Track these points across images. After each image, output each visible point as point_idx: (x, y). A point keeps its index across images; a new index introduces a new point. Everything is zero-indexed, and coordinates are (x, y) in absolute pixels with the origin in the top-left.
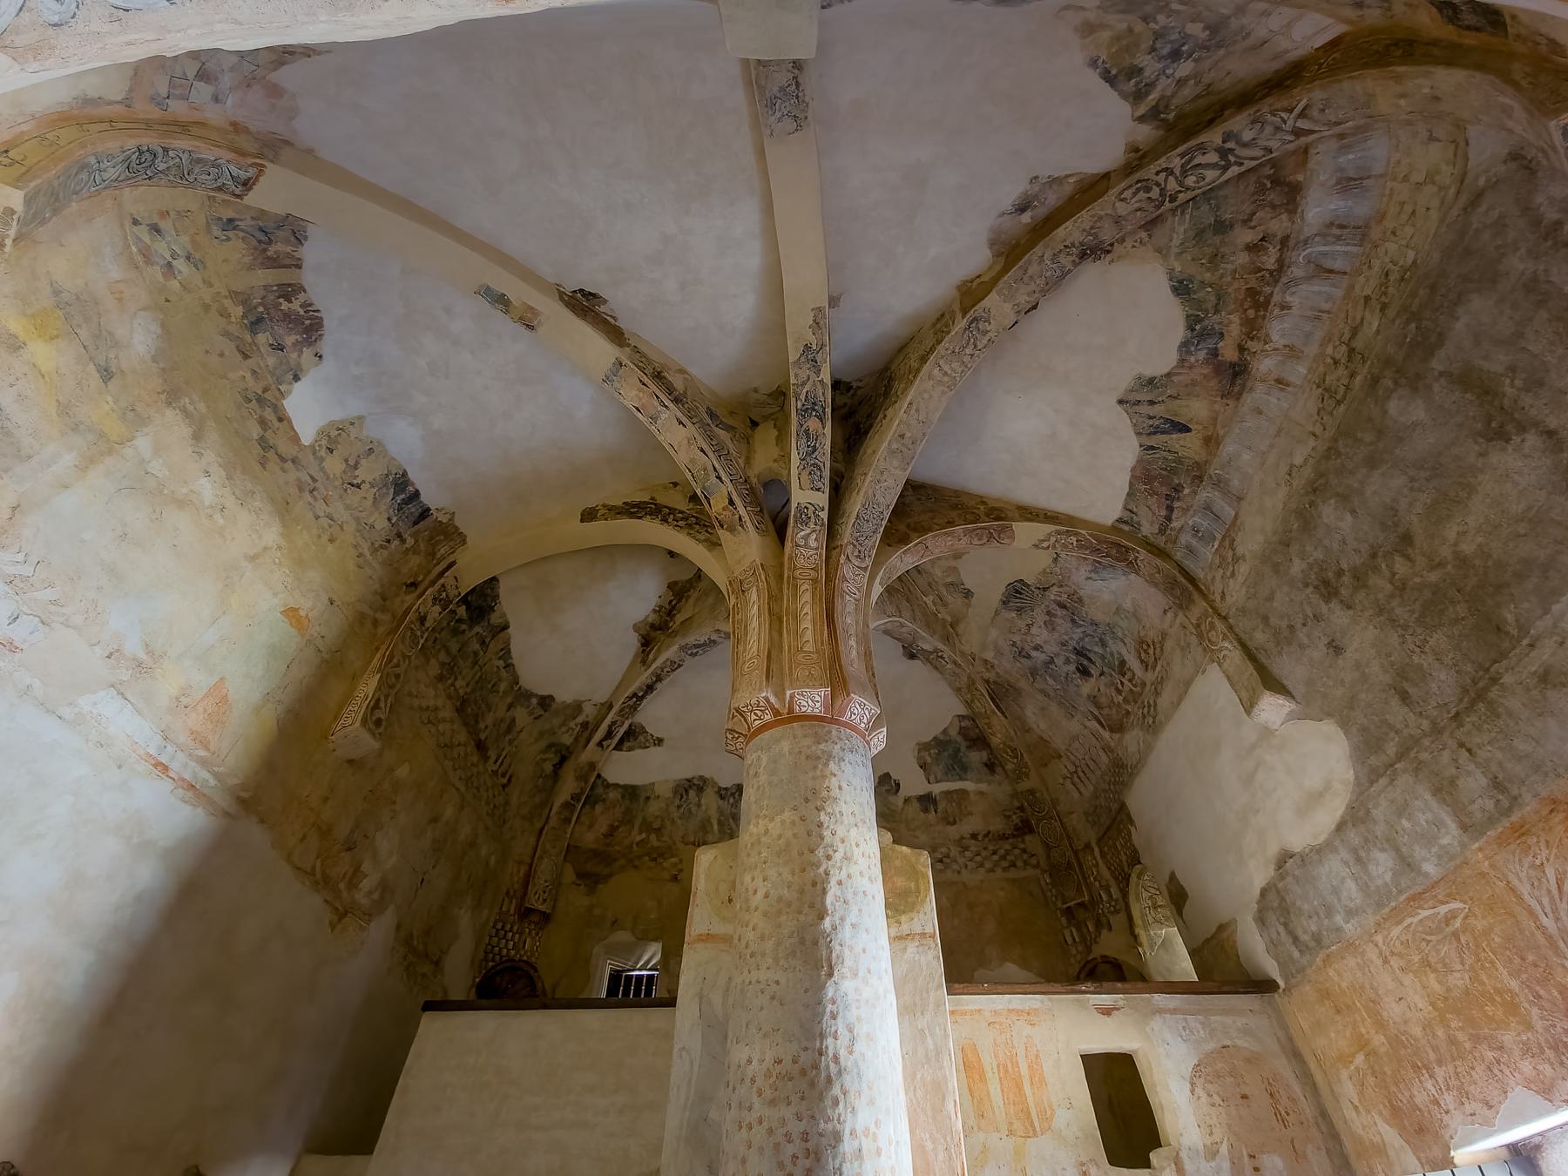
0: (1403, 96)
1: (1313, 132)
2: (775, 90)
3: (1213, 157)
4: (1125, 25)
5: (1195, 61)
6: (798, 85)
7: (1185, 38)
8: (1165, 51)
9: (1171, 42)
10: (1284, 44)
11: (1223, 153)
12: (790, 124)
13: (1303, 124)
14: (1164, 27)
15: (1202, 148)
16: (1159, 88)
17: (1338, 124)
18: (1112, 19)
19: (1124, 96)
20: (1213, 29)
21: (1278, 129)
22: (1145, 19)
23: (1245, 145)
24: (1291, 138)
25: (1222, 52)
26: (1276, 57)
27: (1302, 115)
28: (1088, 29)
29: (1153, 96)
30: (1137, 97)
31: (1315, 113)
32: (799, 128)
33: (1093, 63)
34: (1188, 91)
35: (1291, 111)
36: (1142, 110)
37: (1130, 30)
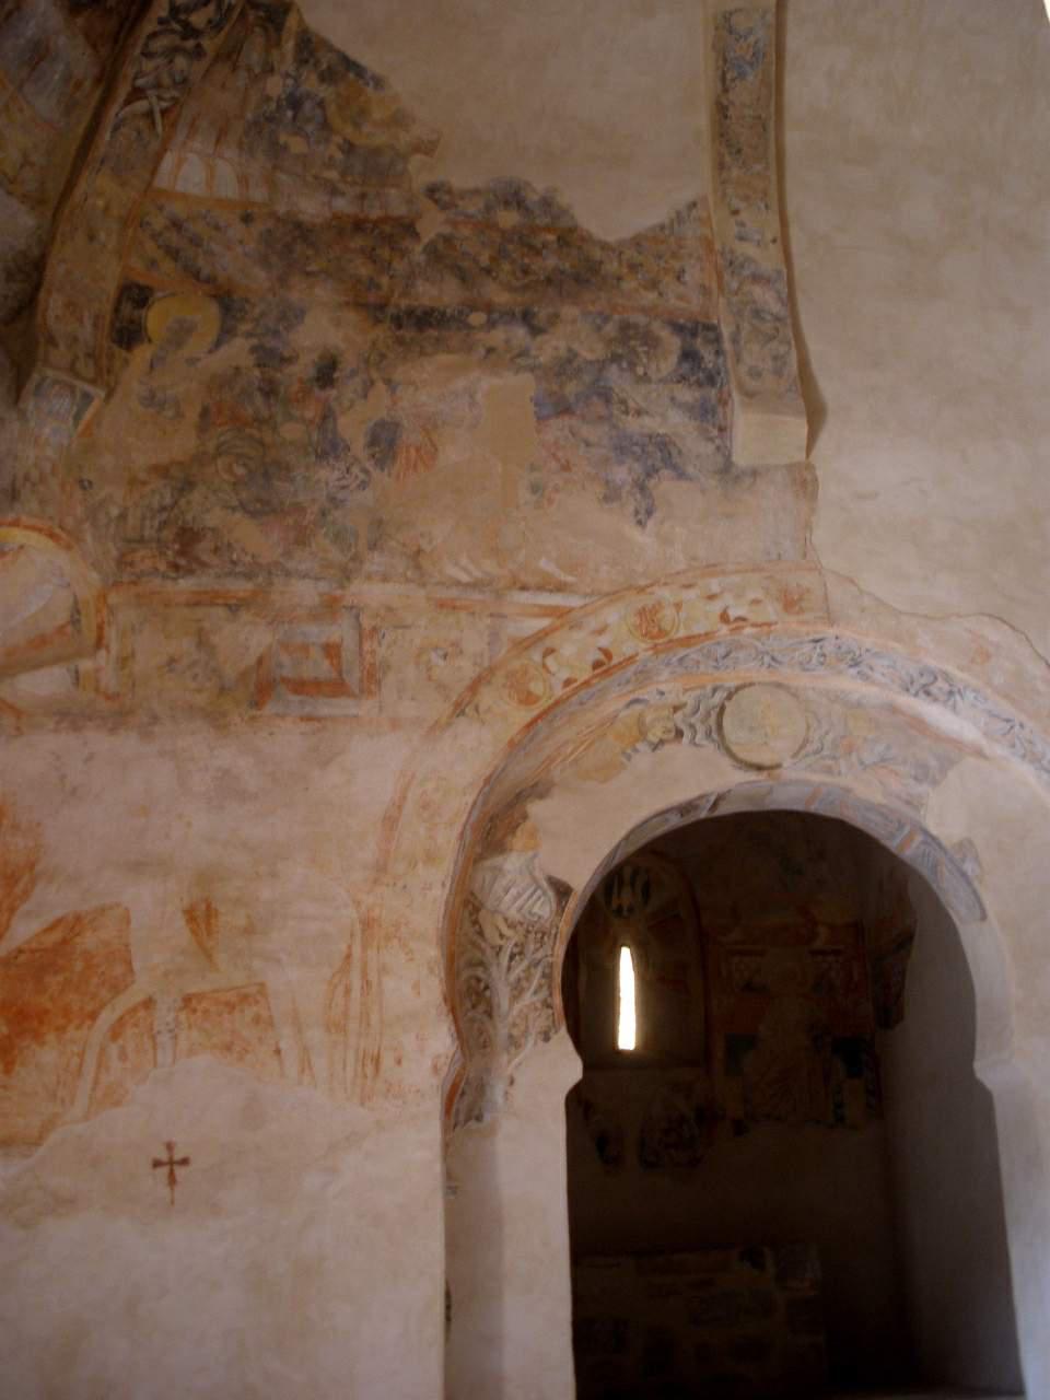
0: (107, 209)
1: (128, 102)
2: (750, 78)
3: (198, 19)
4: (366, 129)
5: (268, 99)
6: (723, 79)
7: (298, 131)
8: (307, 106)
9: (309, 120)
10: (196, 144)
11: (190, 31)
12: (740, 23)
13: (141, 106)
14: (327, 141)
15: (215, 26)
16: (290, 57)
17: (116, 128)
18: (381, 139)
19: (326, 44)
20: (277, 150)
21: (158, 85)
22: (349, 148)
23: (176, 50)
24: (140, 82)
25: (249, 116)
26: (193, 128)
27: (149, 114)
28: (399, 120)
29: (289, 46)
30: (308, 46)
31: (142, 124)
32: (727, 16)
33: (379, 82)
34: (253, 55)
35: (164, 112)
36: (291, 22)
37: (357, 125)
